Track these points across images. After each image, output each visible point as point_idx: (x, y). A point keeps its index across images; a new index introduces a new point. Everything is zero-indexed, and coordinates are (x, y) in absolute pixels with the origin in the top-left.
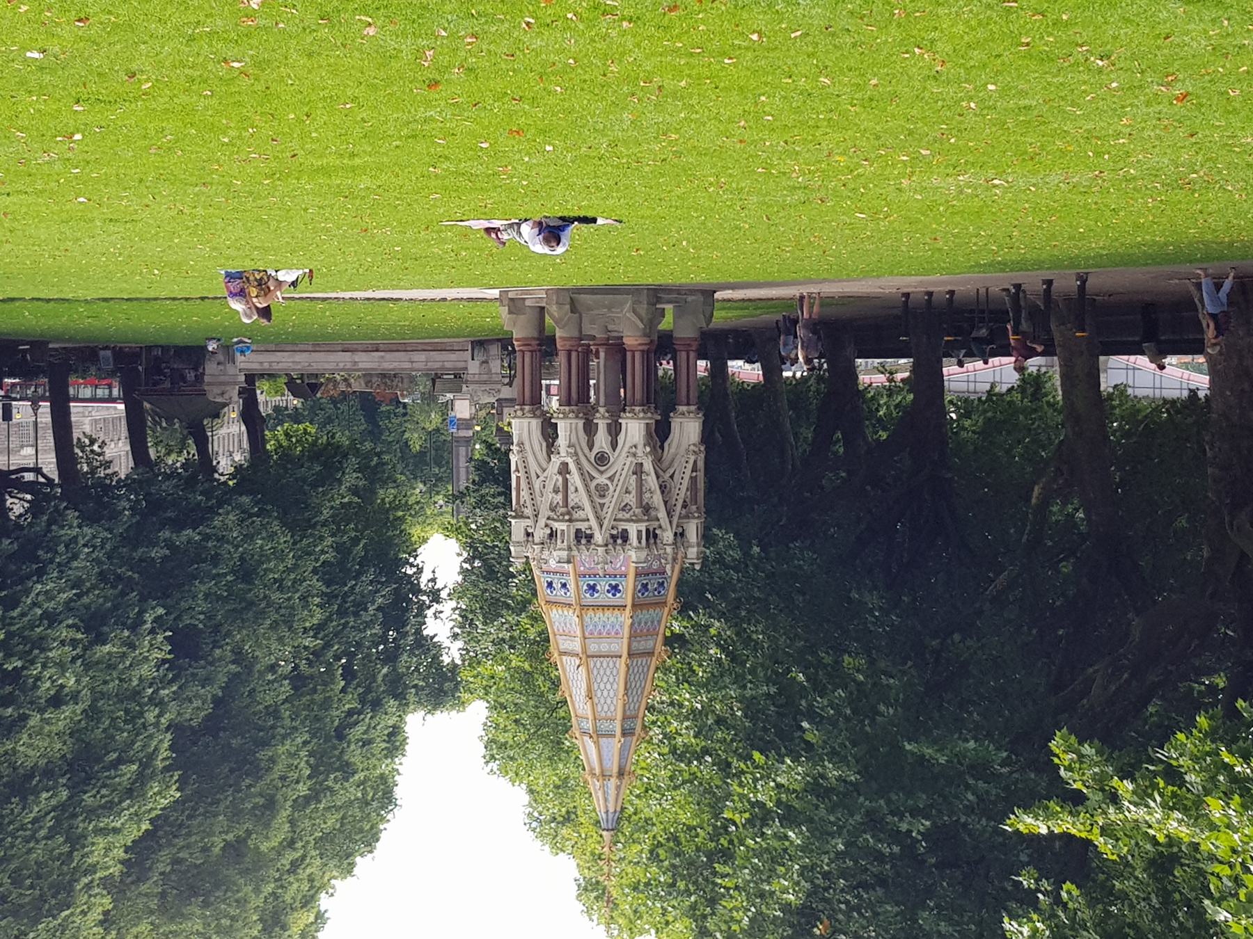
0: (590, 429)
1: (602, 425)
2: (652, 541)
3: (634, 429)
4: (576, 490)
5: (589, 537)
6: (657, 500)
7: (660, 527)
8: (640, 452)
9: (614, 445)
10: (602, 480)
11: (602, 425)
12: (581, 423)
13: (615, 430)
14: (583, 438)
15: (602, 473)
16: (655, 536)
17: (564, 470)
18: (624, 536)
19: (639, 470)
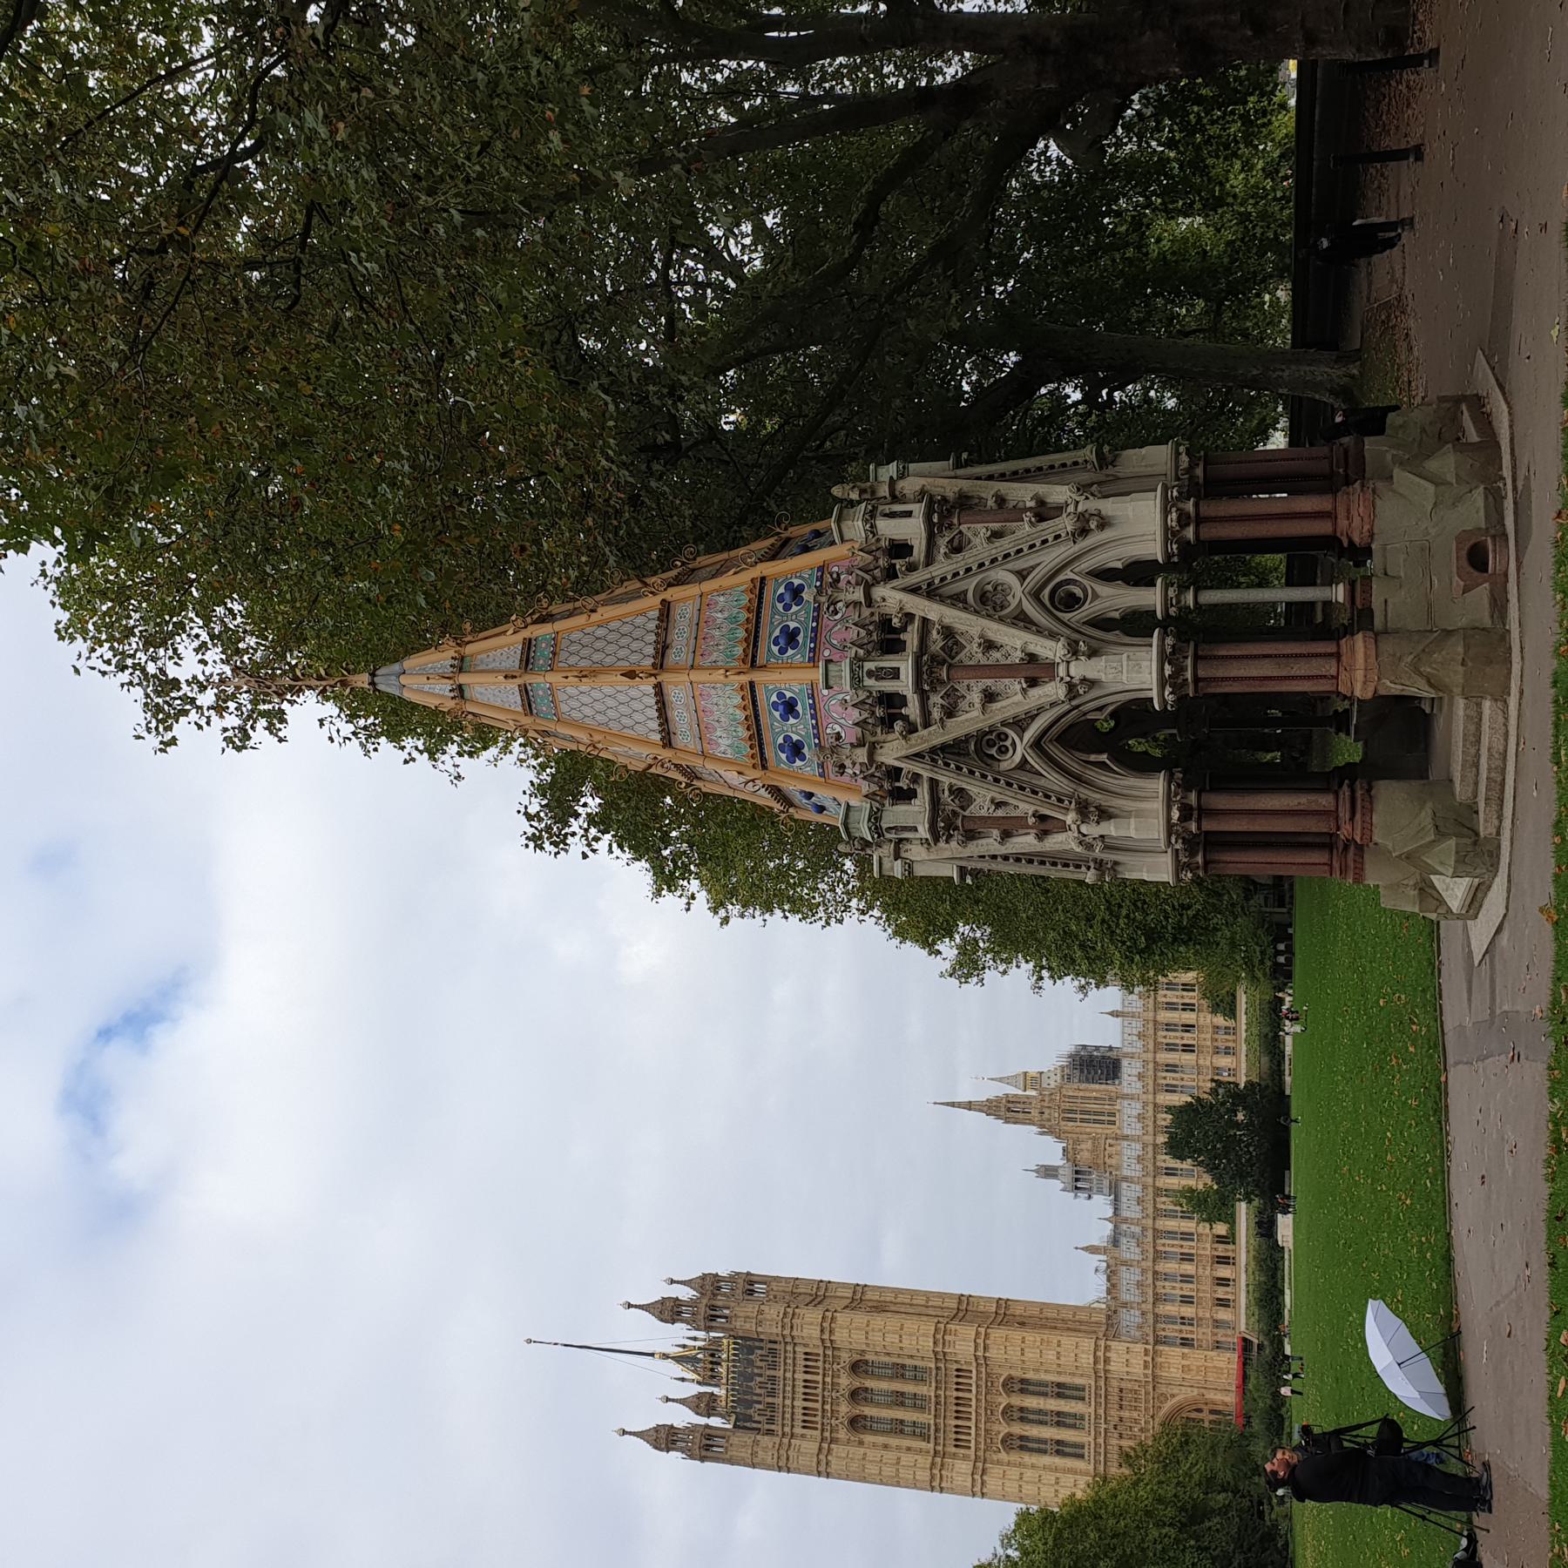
0: (1137, 573)
1: (1151, 598)
2: (879, 712)
3: (1135, 672)
4: (996, 535)
5: (891, 574)
6: (971, 719)
7: (911, 729)
8: (1080, 669)
9: (1102, 623)
10: (1018, 594)
11: (1151, 598)
12: (1153, 549)
13: (1135, 625)
14: (1113, 558)
15: (1036, 595)
16: (888, 723)
17: (1043, 511)
18: (891, 645)
19: (1034, 671)
